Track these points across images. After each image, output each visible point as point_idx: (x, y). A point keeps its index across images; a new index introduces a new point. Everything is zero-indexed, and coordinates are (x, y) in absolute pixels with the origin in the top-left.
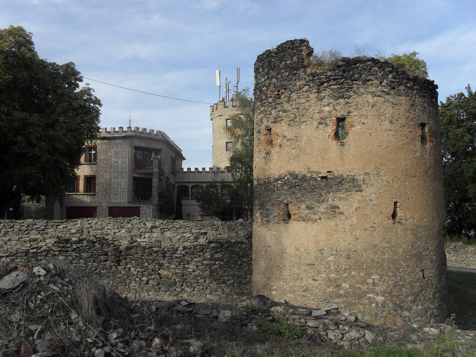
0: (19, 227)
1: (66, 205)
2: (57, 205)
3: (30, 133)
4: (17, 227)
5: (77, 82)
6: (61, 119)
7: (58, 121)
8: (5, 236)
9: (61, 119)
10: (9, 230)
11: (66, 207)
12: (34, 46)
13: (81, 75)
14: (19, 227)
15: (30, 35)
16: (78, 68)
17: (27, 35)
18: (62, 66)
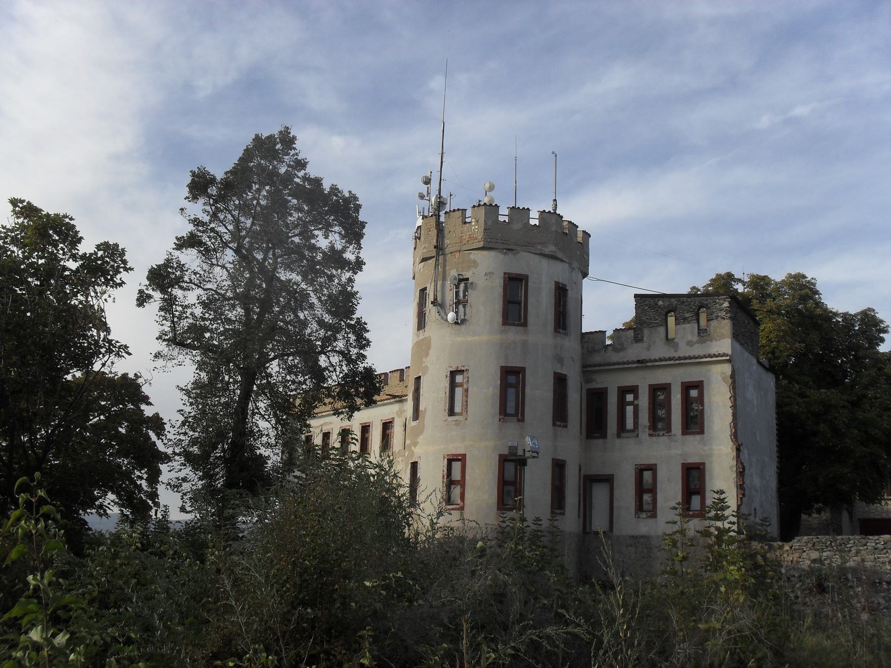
0: (874, 544)
1: (858, 517)
2: (845, 515)
3: (836, 418)
4: (871, 544)
5: (881, 335)
6: (870, 393)
7: (865, 396)
8: (856, 556)
9: (870, 393)
10: (861, 548)
11: (859, 519)
12: (821, 296)
13: (886, 324)
14: (874, 544)
15: (813, 281)
16: (880, 316)
17: (809, 282)
18: (856, 315)
